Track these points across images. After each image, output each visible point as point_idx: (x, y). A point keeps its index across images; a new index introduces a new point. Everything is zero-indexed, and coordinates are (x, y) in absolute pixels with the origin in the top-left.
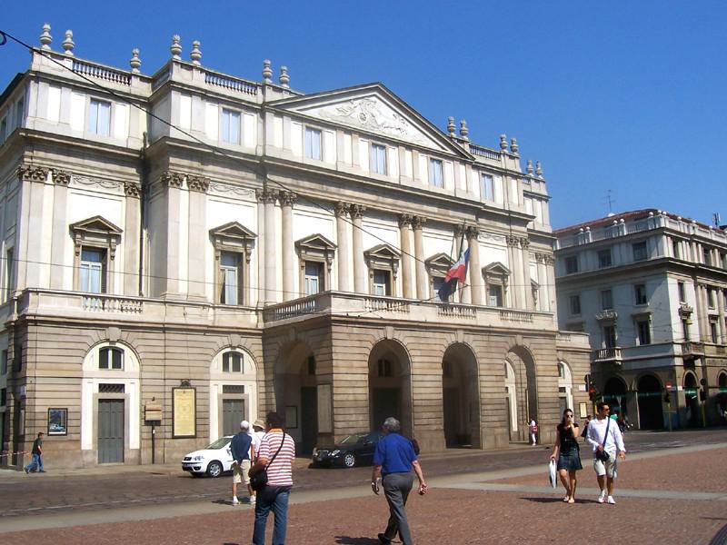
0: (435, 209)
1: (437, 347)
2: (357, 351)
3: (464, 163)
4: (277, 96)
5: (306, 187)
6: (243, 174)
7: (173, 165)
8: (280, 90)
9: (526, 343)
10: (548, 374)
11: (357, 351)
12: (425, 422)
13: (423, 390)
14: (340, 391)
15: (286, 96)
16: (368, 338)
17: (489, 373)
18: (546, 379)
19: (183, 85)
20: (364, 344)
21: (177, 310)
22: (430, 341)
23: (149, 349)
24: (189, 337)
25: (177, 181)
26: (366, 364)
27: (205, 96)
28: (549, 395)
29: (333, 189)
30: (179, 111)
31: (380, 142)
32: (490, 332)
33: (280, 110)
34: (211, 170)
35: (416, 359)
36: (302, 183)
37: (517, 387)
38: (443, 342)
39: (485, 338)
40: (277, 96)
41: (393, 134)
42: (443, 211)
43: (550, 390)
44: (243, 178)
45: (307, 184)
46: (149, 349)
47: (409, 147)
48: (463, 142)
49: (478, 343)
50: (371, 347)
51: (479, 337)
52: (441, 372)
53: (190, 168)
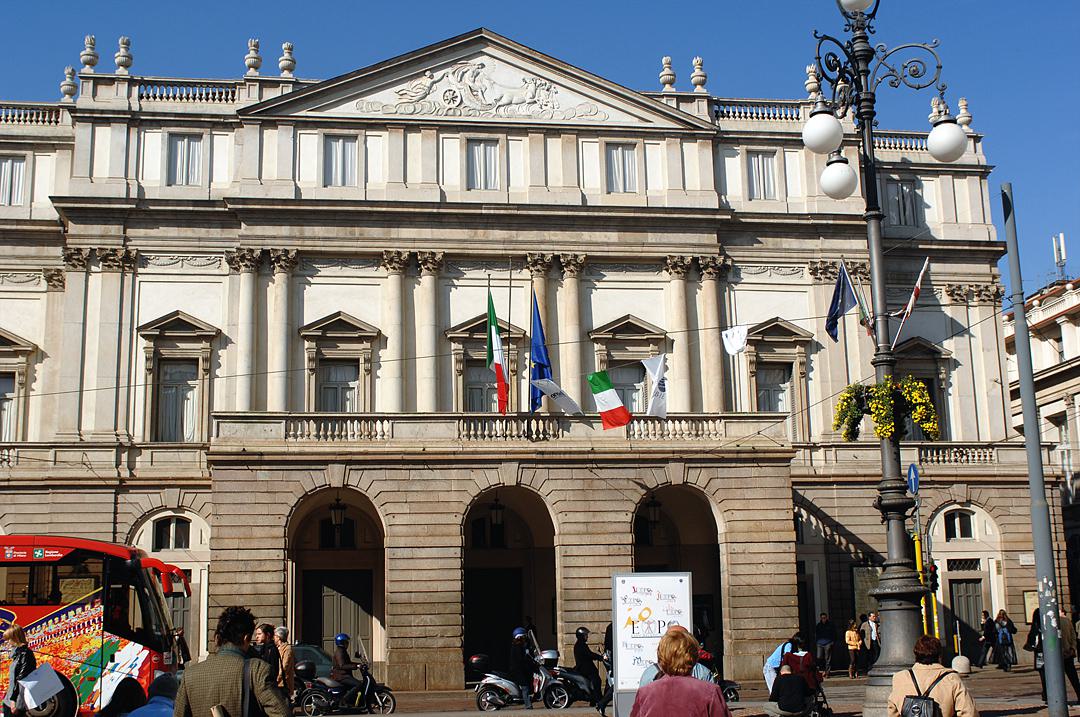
0: (613, 236)
1: (454, 497)
2: (264, 510)
3: (693, 138)
4: (270, 94)
5: (318, 236)
6: (201, 232)
7: (73, 236)
8: (275, 84)
9: (698, 478)
10: (755, 537)
11: (264, 510)
12: (416, 632)
13: (414, 575)
14: (222, 578)
15: (289, 90)
16: (292, 487)
17: (586, 539)
18: (755, 548)
19: (92, 111)
20: (279, 498)
21: (74, 456)
22: (433, 486)
23: (21, 519)
24: (89, 498)
25: (82, 261)
26: (280, 532)
27: (136, 121)
28: (766, 580)
29: (376, 232)
30: (163, 143)
31: (480, 133)
32: (591, 461)
33: (266, 116)
34: (141, 238)
35: (399, 520)
36: (309, 231)
37: (827, 560)
38: (463, 488)
39: (587, 474)
40: (270, 94)
41: (521, 114)
42: (630, 237)
43: (771, 569)
44: (200, 239)
45: (319, 231)
46: (21, 519)
47: (552, 131)
48: (690, 99)
49: (559, 485)
50: (293, 501)
51: (566, 473)
52: (458, 541)
53: (102, 237)
